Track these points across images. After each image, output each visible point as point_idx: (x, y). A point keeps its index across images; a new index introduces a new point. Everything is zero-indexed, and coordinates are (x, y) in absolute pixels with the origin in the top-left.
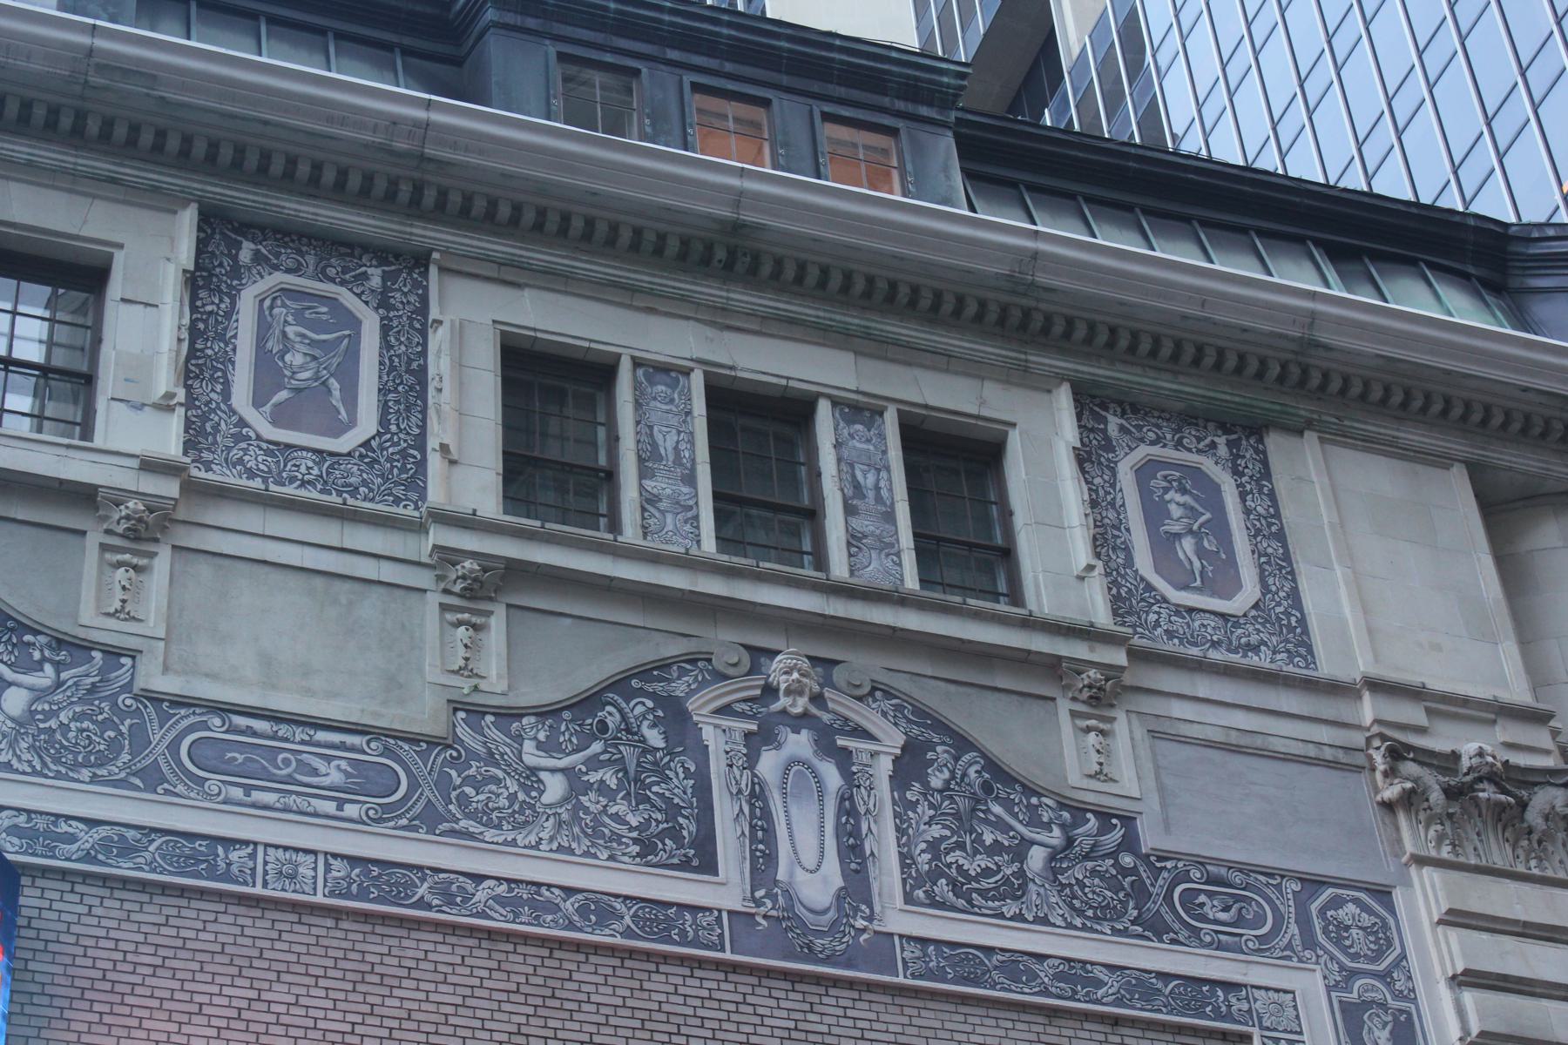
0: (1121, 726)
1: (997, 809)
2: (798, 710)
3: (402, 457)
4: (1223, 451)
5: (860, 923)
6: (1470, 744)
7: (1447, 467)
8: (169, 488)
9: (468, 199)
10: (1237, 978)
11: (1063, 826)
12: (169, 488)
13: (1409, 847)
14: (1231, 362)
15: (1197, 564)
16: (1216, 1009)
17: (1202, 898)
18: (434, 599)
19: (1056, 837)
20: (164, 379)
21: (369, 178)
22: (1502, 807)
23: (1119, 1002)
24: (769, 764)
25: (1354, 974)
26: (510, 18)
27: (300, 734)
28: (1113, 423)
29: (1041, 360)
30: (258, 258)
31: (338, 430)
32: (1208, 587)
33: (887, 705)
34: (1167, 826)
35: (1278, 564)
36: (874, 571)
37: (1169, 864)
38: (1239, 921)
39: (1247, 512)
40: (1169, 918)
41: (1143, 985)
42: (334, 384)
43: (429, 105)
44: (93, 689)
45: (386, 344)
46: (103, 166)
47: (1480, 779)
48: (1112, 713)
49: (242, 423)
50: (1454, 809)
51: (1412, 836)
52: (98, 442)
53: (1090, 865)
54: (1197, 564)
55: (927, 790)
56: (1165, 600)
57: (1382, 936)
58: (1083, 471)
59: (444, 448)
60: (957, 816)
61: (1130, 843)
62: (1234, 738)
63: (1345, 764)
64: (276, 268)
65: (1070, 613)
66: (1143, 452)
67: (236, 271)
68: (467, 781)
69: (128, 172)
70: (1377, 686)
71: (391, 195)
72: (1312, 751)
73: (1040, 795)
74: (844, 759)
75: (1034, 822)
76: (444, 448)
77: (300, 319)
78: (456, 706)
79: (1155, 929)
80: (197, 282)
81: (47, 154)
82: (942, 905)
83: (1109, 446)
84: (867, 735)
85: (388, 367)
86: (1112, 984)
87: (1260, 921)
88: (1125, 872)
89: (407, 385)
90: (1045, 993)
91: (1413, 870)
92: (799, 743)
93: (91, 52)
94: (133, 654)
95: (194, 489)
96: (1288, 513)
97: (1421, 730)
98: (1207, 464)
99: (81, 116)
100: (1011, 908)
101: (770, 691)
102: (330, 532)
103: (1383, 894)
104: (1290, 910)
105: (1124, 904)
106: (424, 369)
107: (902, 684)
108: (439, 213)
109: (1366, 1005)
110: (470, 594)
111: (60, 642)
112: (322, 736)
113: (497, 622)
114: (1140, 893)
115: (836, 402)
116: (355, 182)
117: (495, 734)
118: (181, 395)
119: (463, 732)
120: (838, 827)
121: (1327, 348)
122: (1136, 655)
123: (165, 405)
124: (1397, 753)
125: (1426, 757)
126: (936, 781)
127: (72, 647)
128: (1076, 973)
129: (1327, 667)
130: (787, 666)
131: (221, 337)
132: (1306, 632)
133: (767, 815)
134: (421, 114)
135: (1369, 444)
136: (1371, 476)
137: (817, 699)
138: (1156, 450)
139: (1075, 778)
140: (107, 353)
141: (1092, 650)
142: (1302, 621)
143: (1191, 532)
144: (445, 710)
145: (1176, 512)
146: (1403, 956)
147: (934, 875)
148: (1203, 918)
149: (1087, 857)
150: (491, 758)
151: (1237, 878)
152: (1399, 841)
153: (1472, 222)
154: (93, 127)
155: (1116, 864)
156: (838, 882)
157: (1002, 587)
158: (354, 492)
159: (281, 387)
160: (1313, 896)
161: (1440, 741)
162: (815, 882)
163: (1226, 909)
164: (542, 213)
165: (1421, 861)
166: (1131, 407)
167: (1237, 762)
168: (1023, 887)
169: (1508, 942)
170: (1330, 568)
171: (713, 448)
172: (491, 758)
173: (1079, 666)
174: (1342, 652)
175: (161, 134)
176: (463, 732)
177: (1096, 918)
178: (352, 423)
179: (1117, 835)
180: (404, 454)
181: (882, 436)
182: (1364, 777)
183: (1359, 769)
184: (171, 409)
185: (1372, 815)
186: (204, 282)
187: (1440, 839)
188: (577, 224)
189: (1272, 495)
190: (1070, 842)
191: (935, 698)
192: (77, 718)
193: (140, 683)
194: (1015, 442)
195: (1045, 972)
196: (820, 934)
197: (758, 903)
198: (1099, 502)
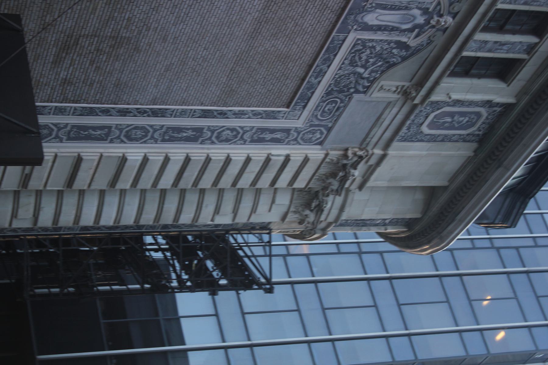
0: (395, 96)
1: (380, 64)
2: (432, 22)
4: (477, 133)
5: (355, 27)
6: (357, 173)
7: (449, 181)
10: (307, 108)
16: (299, 103)
17: (334, 105)
19: (366, 75)
23: (308, 82)
24: (417, 12)
28: (498, 109)
29: (526, 98)
32: (432, 122)
33: (425, 43)
35: (433, 139)
36: (471, 44)
37: (347, 99)
38: (324, 111)
39: (454, 135)
40: (331, 97)
41: (312, 88)
47: (346, 173)
48: (401, 93)
50: (340, 164)
51: (334, 154)
53: (354, 82)
55: (394, 48)
56: (433, 112)
57: (308, 141)
60: (381, 54)
61: (357, 92)
62: (381, 120)
63: (363, 144)
65: (438, 89)
70: (383, 157)
72: (370, 136)
73: (381, 74)
74: (411, 30)
75: (372, 71)
79: (328, 93)
82: (354, 46)
84: (416, 36)
87: (322, 116)
90: (317, 66)
91: (325, 152)
92: (421, 20)
96: (449, 144)
97: (367, 162)
100: (347, 62)
101: (441, 16)
103: (321, 143)
104: (323, 123)
107: (430, 48)
109: (289, 134)
115: (536, 44)
120: (389, 26)
121: (497, 168)
122: (416, 106)
124: (361, 158)
126: (395, 51)
128: (321, 74)
129: (395, 144)
130: (448, 20)
132: (409, 141)
133: (399, 9)
135: (463, 167)
136: (453, 166)
137: (433, 27)
138: (484, 118)
139: (382, 83)
141: (422, 96)
142: (412, 141)
145: (461, 119)
146: (300, 144)
147: (364, 46)
148: (327, 104)
149: (356, 82)
151: (337, 113)
153: (538, 188)
155: (351, 88)
156: (370, 23)
157: (457, 69)
160: (325, 129)
161: (362, 167)
162: (371, 19)
163: (329, 110)
165: (327, 155)
167: (373, 119)
168: (352, 66)
170: (427, 150)
171: (532, 12)
177: (336, 80)
179: (360, 88)
181: (519, 53)
182: (358, 145)
183: (361, 144)
185: (345, 146)
187: (332, 160)
190: (363, 78)
191: (422, 55)
194: (502, 85)
195: (324, 67)
196: (355, 17)
197: (371, 4)
198: (471, 103)
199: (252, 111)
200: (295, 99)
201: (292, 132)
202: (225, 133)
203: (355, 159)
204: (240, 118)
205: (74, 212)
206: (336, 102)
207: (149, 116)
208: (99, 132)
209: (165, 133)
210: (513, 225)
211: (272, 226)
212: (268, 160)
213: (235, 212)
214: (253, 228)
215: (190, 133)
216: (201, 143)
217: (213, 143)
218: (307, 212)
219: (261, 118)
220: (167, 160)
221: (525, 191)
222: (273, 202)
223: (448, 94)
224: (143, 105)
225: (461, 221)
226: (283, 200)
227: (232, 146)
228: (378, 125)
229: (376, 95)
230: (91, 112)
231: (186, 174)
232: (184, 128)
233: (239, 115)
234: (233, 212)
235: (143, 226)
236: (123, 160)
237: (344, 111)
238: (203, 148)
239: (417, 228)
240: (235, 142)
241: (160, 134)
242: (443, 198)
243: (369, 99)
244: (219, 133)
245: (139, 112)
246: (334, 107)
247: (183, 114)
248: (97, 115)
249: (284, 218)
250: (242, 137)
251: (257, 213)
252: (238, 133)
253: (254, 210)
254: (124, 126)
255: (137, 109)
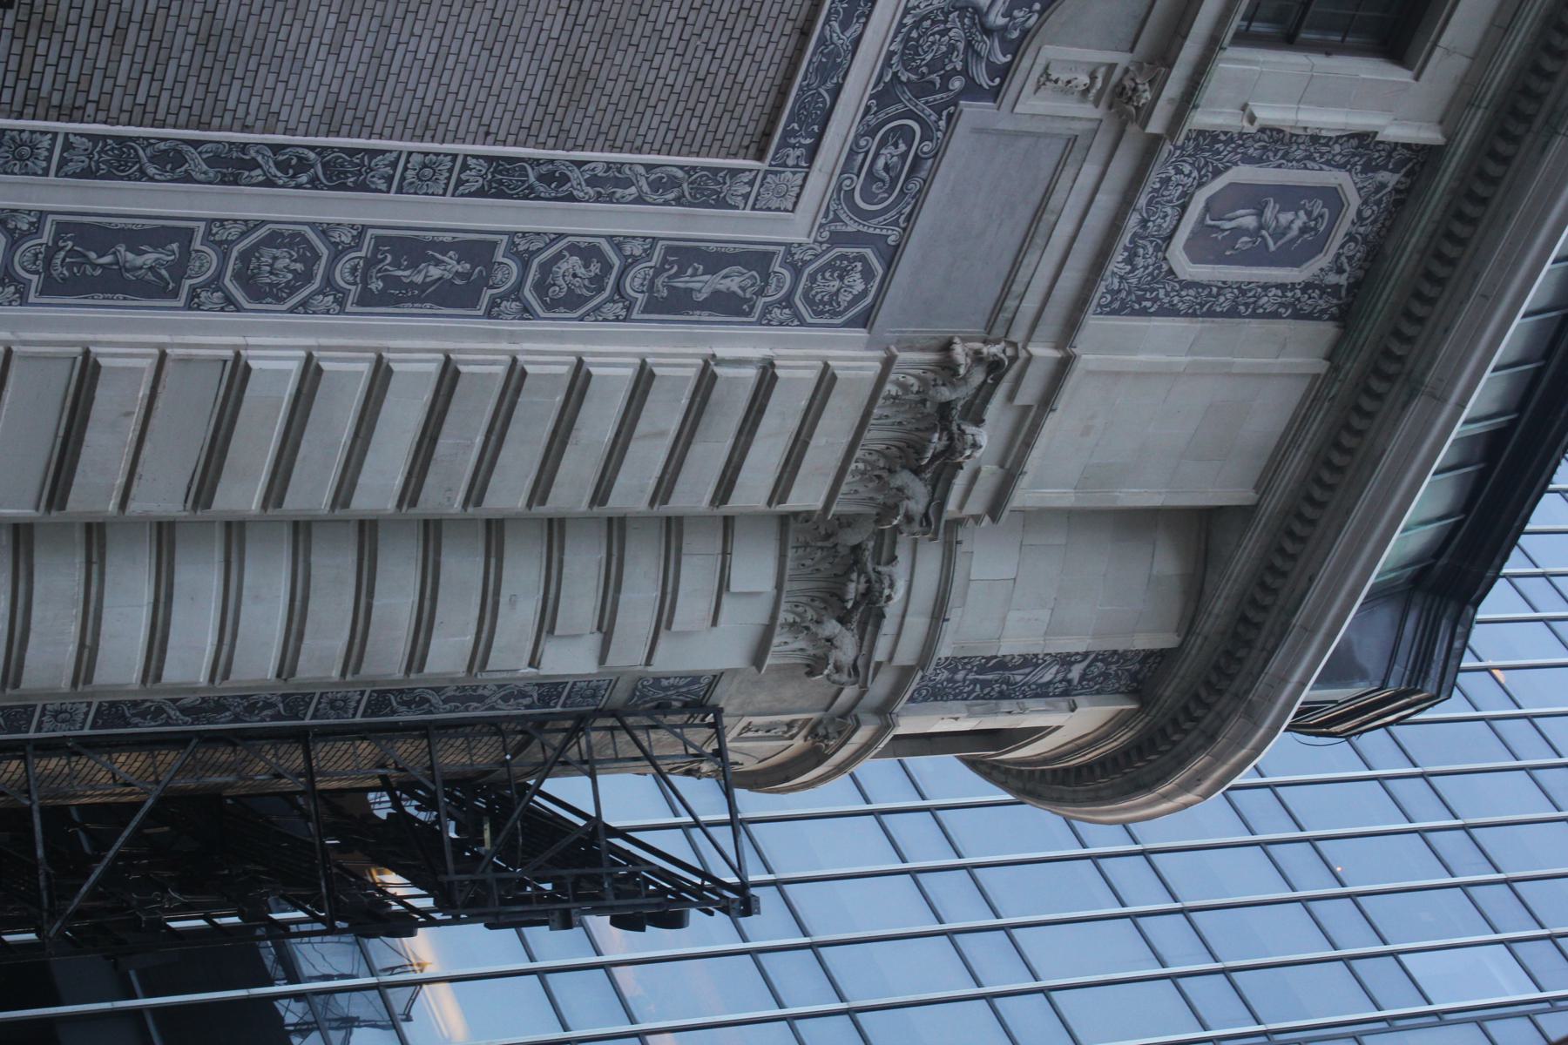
0: (1088, 111)
4: (1332, 279)
6: (988, 437)
7: (1257, 487)
10: (819, 161)
11: (1005, 28)
13: (903, 356)
14: (1418, 309)
15: (1227, 225)
16: (794, 133)
17: (902, 147)
22: (920, 452)
23: (822, 41)
25: (797, 271)
28: (1390, 178)
32: (1202, 231)
34: (979, 131)
35: (1205, 304)
37: (942, 123)
38: (872, 177)
39: (1266, 287)
40: (892, 110)
41: (834, 68)
47: (951, 438)
48: (1103, 105)
51: (913, 360)
53: (961, 46)
54: (1227, 225)
56: (1200, 185)
57: (826, 309)
58: (1352, 136)
61: (973, 91)
62: (1048, 217)
63: (997, 318)
65: (1213, 87)
66: (1354, 200)
70: (1063, 367)
72: (1017, 288)
73: (1041, 13)
79: (884, 95)
83: (1368, 168)
86: (842, 39)
87: (868, 197)
88: (946, 78)
91: (881, 354)
96: (1254, 325)
97: (1011, 397)
98: (1323, 261)
103: (865, 320)
105: (915, 70)
109: (766, 276)
114: (922, 88)
121: (1405, 406)
122: (1155, 142)
124: (996, 368)
125: (984, 395)
129: (1095, 324)
132: (1134, 313)
135: (1299, 421)
136: (1267, 414)
138: (1351, 214)
139: (1049, 52)
141: (1171, 100)
142: (1144, 312)
143: (1261, 227)
145: (1285, 218)
146: (803, 323)
148: (883, 143)
149: (969, 45)
151: (914, 186)
152: (911, 348)
153: (1490, 574)
155: (955, 72)
157: (1257, 27)
160: (879, 255)
161: (997, 412)
163: (887, 168)
165: (888, 363)
166: (1402, 201)
167: (1025, 213)
169: (793, 424)
170: (1190, 352)
173: (1158, 84)
174: (1106, 343)
177: (907, 39)
179: (983, 79)
182: (979, 331)
183: (990, 327)
185: (943, 330)
187: (905, 387)
189: (1275, 315)
190: (988, 31)
194: (1401, 75)
198: (1315, 145)
199: (649, 167)
200: (782, 123)
201: (776, 266)
202: (564, 266)
203: (978, 377)
204: (611, 199)
205: (74, 629)
206: (907, 134)
207: (314, 183)
208: (150, 258)
209: (371, 262)
210: (1445, 689)
211: (721, 697)
212: (706, 380)
213: (606, 627)
214: (663, 707)
215: (452, 265)
216: (488, 315)
217: (526, 312)
218: (832, 627)
219: (679, 201)
220: (381, 374)
221: (1452, 579)
222: (723, 585)
223: (1244, 108)
224: (294, 132)
225: (1309, 630)
226: (756, 570)
227: (589, 326)
228: (1039, 241)
229: (1033, 105)
230: (118, 161)
231: (444, 444)
232: (434, 245)
233: (608, 184)
234: (599, 628)
235: (306, 699)
236: (238, 373)
237: (934, 172)
238: (495, 335)
239: (1169, 693)
240: (597, 308)
241: (354, 270)
242: (1244, 556)
243: (1006, 124)
244: (546, 268)
245: (282, 166)
246: (904, 156)
247: (426, 176)
248: (143, 175)
249: (758, 658)
250: (618, 288)
251: (674, 628)
252: (607, 267)
253: (664, 618)
254: (235, 231)
255: (277, 148)
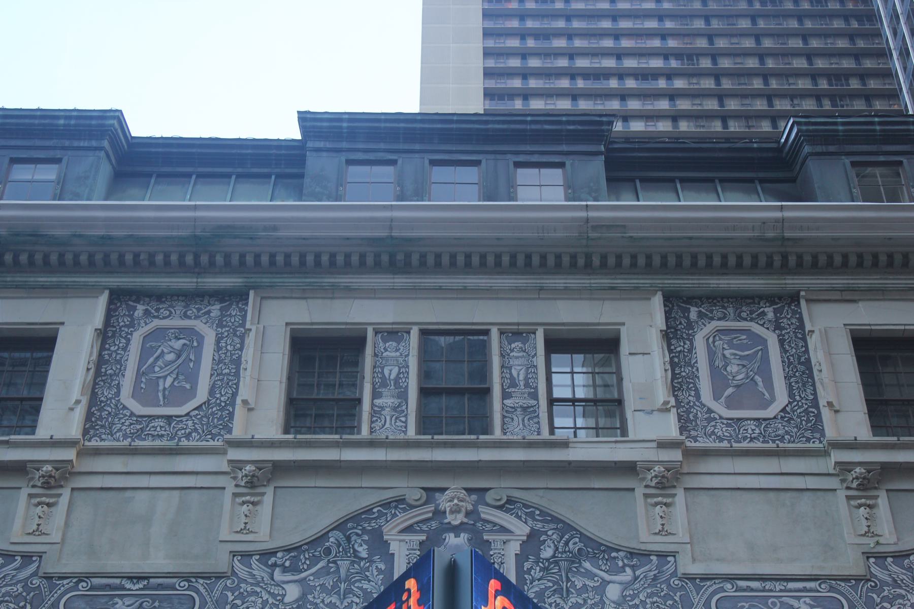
3: (806, 413)
8: (676, 455)
9: (815, 257)
12: (676, 455)
18: (842, 494)
20: (662, 394)
21: (755, 257)
26: (819, 149)
27: (779, 586)
30: (701, 315)
31: (766, 405)
42: (758, 379)
43: (782, 208)
44: (655, 578)
45: (783, 350)
46: (606, 281)
49: (710, 411)
52: (631, 436)
59: (830, 404)
64: (712, 319)
67: (690, 325)
68: (883, 599)
69: (619, 282)
71: (770, 264)
76: (830, 404)
77: (732, 346)
78: (868, 555)
80: (670, 335)
81: (574, 281)
85: (787, 363)
89: (801, 371)
93: (587, 220)
94: (674, 554)
95: (690, 454)
99: (588, 257)
102: (771, 465)
106: (808, 360)
108: (800, 269)
110: (862, 487)
111: (632, 554)
112: (791, 585)
113: (883, 501)
116: (747, 261)
117: (895, 568)
118: (673, 402)
119: (875, 570)
123: (664, 409)
127: (639, 555)
131: (689, 364)
134: (778, 214)
140: (626, 384)
144: (861, 560)
150: (895, 584)
154: (596, 261)
158: (782, 439)
159: (728, 386)
164: (860, 256)
172: (895, 584)
175: (634, 257)
176: (875, 570)
178: (773, 399)
180: (806, 412)
184: (668, 410)
186: (674, 335)
188: (883, 259)
192: (649, 596)
193: (681, 571)
